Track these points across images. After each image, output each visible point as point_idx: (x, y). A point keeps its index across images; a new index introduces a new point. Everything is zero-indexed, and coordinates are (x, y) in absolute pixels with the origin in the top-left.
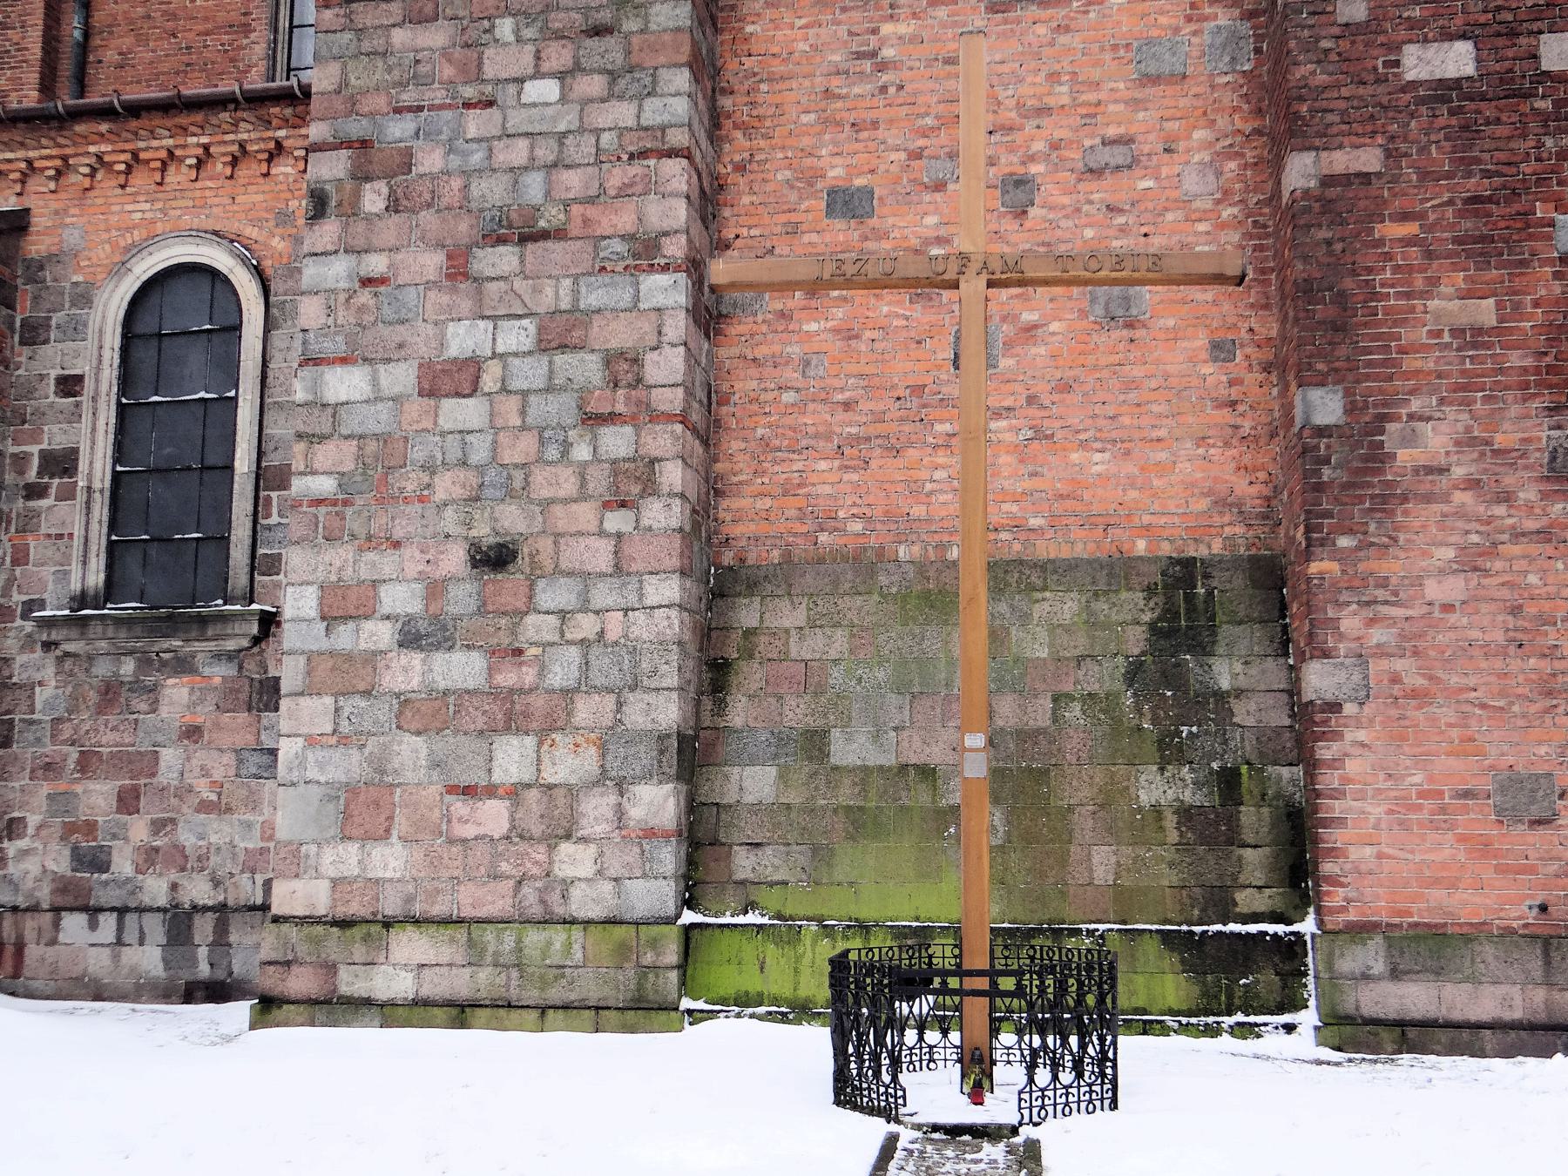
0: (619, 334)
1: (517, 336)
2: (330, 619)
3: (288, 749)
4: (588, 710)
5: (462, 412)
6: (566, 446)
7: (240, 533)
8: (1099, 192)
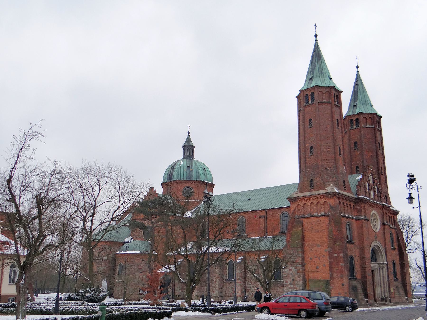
1: (294, 268)
3: (284, 290)
4: (298, 288)
5: (291, 272)
7: (281, 276)
8: (323, 258)
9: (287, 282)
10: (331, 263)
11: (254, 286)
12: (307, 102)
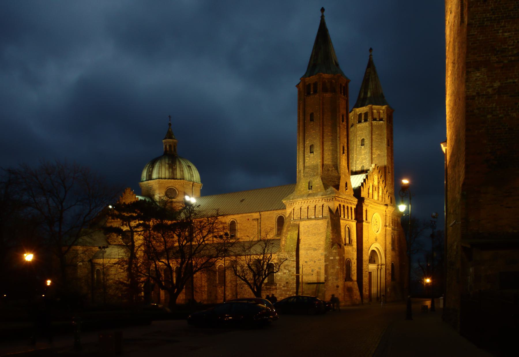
0: (292, 271)
2: (279, 286)
5: (285, 275)
6: (290, 277)
8: (319, 262)
9: (280, 285)
10: (326, 266)
11: (246, 290)
12: (309, 94)
